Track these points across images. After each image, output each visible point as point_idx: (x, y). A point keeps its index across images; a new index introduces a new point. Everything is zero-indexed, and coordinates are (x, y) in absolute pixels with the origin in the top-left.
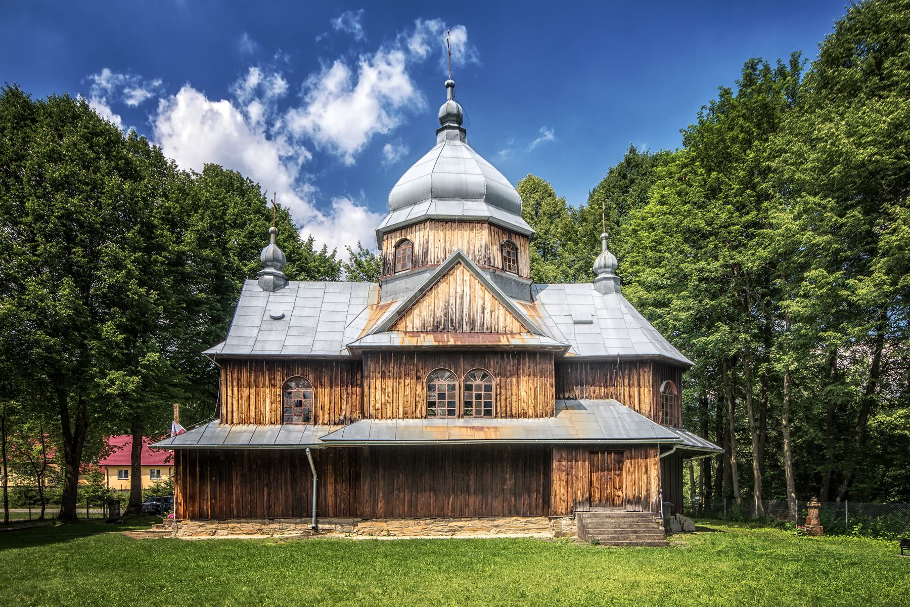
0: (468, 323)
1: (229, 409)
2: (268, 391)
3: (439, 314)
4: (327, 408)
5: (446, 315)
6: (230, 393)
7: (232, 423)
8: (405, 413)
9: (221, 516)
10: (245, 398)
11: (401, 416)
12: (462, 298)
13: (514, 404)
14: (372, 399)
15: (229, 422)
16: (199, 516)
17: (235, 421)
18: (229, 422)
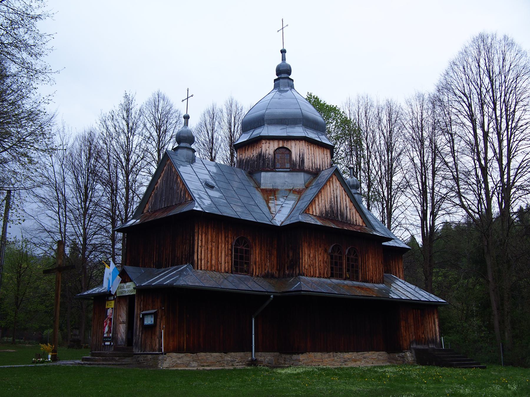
0: (340, 215)
1: (199, 257)
2: (223, 246)
3: (328, 207)
4: (257, 264)
5: (331, 207)
6: (200, 244)
7: (201, 269)
8: (320, 274)
9: (193, 349)
10: (209, 250)
11: (317, 275)
12: (337, 197)
13: (367, 273)
14: (304, 261)
15: (199, 269)
16: (179, 350)
17: (203, 269)
18: (199, 269)
